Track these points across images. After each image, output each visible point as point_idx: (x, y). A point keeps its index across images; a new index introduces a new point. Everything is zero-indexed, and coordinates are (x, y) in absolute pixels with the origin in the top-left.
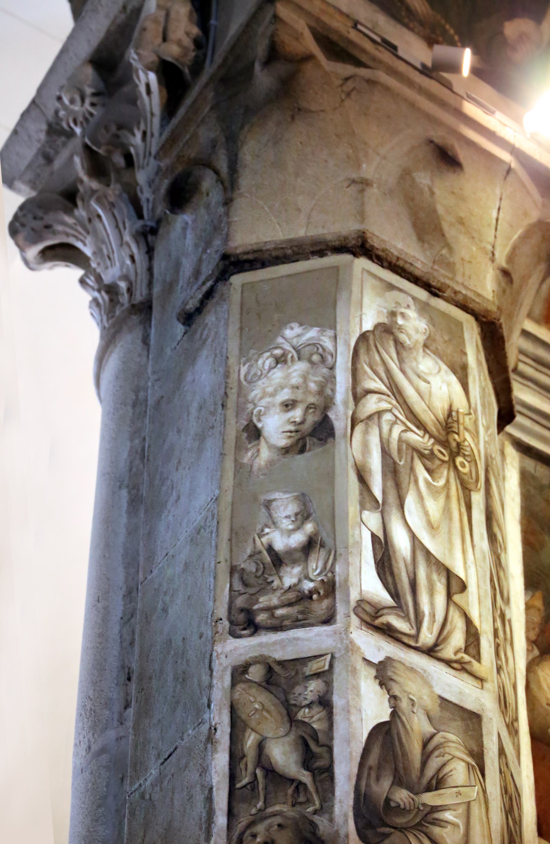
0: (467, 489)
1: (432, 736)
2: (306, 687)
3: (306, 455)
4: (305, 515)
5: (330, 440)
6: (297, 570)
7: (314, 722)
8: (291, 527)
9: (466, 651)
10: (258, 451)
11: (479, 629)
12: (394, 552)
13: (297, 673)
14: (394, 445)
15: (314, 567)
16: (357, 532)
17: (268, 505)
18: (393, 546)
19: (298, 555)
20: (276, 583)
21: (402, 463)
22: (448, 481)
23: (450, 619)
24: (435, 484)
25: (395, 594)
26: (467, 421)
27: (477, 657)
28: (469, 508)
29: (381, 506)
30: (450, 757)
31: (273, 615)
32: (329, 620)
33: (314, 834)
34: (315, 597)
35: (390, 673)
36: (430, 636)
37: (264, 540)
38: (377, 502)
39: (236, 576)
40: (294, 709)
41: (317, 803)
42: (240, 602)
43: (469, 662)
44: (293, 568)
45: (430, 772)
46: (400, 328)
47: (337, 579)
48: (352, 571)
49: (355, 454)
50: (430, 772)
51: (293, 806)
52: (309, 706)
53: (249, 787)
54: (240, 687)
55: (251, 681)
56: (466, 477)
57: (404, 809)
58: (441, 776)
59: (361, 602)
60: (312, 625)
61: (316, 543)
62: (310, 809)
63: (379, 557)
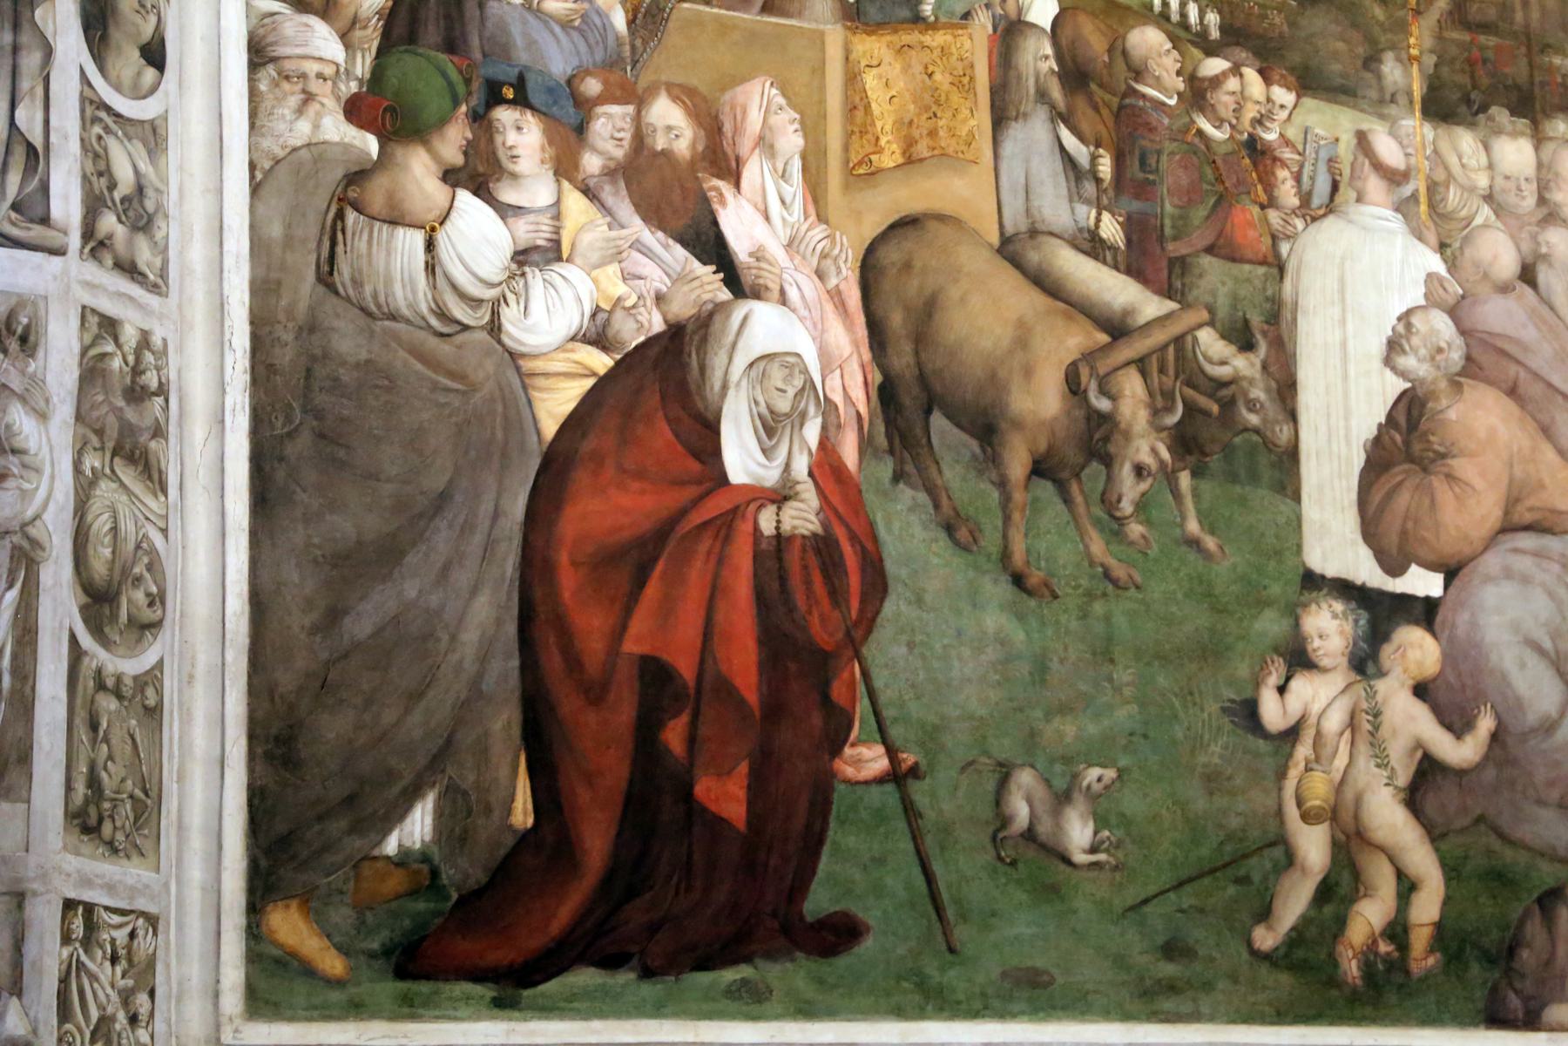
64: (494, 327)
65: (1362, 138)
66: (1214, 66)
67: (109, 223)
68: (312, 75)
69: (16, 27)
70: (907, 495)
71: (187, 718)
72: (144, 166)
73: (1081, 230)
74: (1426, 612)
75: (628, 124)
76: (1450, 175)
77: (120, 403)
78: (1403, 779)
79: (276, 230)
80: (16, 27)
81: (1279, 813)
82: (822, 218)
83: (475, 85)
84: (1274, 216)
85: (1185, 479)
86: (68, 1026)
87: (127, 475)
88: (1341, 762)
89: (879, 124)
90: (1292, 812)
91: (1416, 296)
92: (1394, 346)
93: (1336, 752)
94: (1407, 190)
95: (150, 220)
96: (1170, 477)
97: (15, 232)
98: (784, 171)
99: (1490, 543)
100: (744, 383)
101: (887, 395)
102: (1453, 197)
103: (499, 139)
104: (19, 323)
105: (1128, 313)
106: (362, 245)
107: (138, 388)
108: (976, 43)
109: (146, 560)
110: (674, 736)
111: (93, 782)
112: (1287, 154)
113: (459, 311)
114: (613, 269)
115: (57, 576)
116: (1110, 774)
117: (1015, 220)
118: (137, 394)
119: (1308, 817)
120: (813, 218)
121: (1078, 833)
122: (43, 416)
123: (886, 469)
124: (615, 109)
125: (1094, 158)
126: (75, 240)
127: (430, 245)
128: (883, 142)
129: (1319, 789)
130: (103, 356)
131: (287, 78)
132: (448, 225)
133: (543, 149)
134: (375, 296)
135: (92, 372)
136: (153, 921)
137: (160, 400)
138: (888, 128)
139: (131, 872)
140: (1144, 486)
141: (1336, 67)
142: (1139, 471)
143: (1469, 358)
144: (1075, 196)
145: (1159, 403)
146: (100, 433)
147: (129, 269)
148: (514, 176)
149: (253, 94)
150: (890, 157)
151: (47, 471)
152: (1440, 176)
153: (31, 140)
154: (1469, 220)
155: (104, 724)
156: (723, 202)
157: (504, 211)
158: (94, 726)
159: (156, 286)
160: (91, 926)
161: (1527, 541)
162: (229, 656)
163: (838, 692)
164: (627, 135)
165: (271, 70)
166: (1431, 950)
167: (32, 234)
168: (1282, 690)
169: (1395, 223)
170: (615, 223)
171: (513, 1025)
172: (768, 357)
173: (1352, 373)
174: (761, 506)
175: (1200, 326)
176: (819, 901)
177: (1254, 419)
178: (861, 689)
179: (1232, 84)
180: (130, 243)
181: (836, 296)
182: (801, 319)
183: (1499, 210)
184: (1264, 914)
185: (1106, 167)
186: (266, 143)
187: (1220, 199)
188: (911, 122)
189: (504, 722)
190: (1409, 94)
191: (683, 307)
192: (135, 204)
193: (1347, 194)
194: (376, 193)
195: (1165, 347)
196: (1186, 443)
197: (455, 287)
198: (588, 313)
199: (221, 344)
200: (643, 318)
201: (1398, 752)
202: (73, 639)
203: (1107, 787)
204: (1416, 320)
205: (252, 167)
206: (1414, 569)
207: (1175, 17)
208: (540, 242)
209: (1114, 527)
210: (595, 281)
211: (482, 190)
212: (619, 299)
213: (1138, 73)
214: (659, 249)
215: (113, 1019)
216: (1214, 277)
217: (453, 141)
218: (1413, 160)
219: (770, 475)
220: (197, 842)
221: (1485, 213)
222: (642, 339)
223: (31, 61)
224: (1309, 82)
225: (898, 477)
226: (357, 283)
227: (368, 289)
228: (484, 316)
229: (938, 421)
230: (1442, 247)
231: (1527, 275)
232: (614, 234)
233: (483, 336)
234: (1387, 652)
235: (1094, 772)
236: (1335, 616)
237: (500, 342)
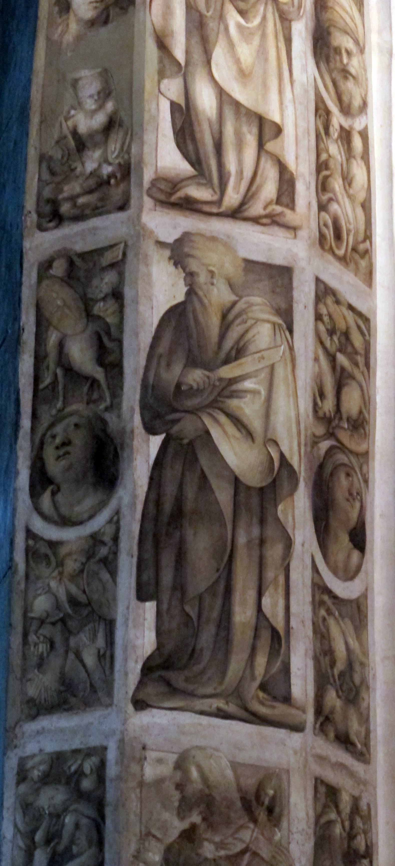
0: (287, 19)
1: (234, 304)
2: (102, 279)
3: (110, 26)
4: (107, 92)
5: (131, 8)
6: (97, 154)
7: (108, 315)
8: (94, 107)
9: (278, 201)
10: (68, 25)
11: (295, 174)
12: (197, 115)
13: (95, 265)
15: (113, 149)
16: (154, 106)
17: (75, 83)
18: (195, 109)
19: (99, 138)
20: (79, 169)
21: (209, 14)
22: (264, 18)
23: (260, 172)
24: (249, 25)
27: (291, 205)
29: (183, 69)
30: (253, 322)
31: (75, 205)
32: (123, 207)
33: (104, 431)
34: (112, 181)
35: (186, 250)
36: (236, 196)
37: (70, 123)
38: (179, 64)
39: (44, 165)
40: (91, 303)
41: (108, 400)
42: (47, 193)
43: (281, 214)
44: (94, 152)
45: (229, 343)
47: (133, 160)
48: (146, 149)
49: (154, 19)
50: (229, 343)
51: (88, 403)
52: (104, 299)
53: (50, 387)
54: (45, 283)
55: (55, 277)
56: (286, 8)
57: (198, 390)
58: (242, 343)
59: (154, 183)
60: (109, 212)
61: (115, 122)
62: (102, 407)
63: (178, 127)
69: (262, 522)
80: (262, 522)
95: (357, 693)
97: (263, 710)
104: (266, 794)
107: (352, 852)
126: (310, 717)
130: (330, 823)
153: (274, 624)
159: (362, 754)
167: (276, 712)
180: (346, 717)
192: (347, 678)
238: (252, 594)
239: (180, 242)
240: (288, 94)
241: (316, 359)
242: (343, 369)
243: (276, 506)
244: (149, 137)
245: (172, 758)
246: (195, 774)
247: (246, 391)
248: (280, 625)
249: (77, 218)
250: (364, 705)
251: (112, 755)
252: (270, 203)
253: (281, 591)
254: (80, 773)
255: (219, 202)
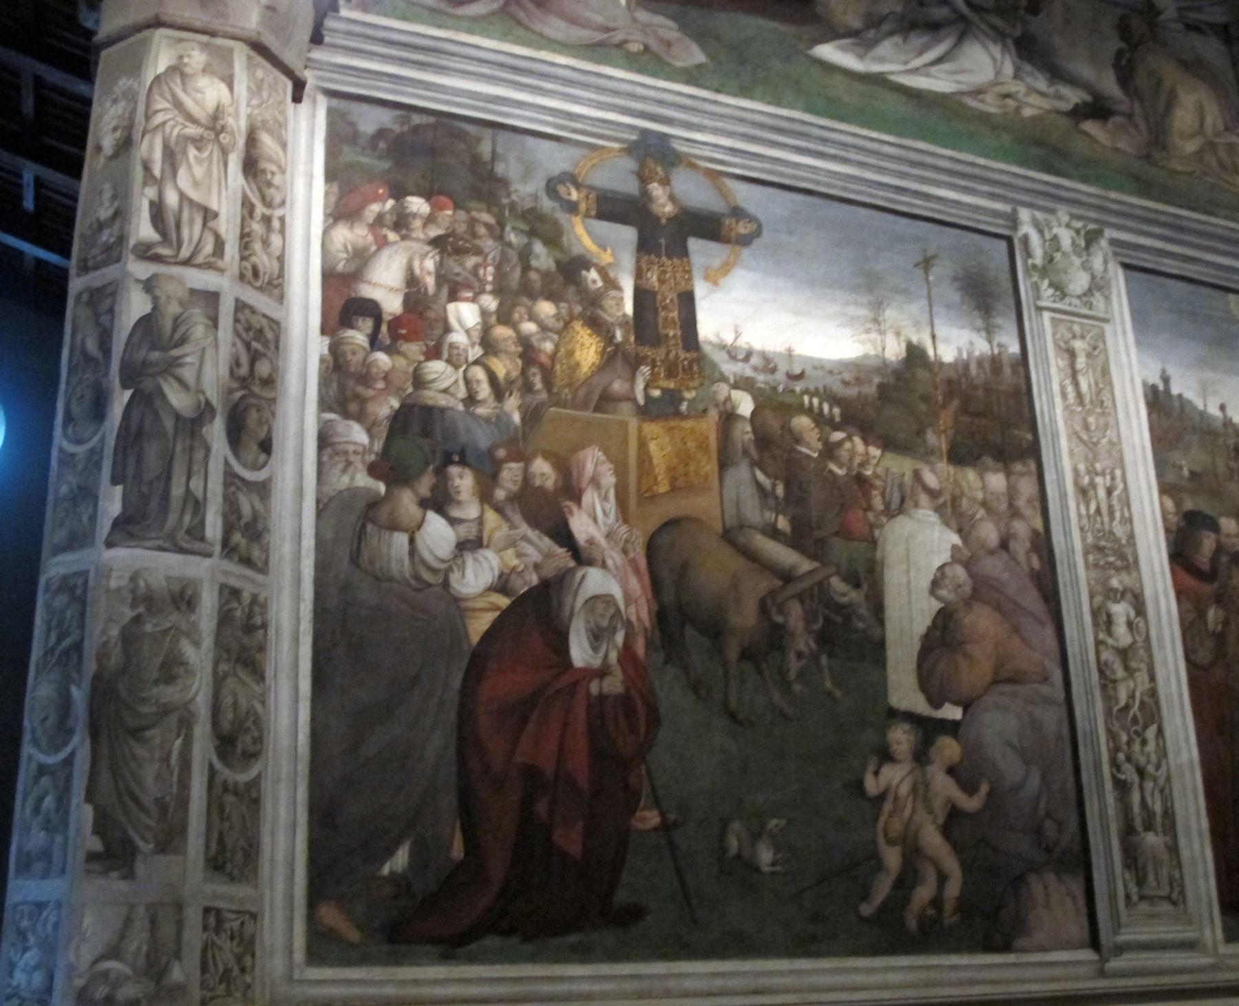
14: (173, 140)
17: (101, 192)
25: (164, 233)
26: (231, 110)
28: (226, 164)
46: (186, 65)
50: (178, 336)
60: (111, 264)
64: (446, 585)
65: (917, 476)
66: (838, 436)
67: (237, 538)
68: (351, 452)
70: (671, 671)
71: (276, 800)
72: (258, 506)
73: (767, 524)
74: (952, 728)
75: (520, 473)
76: (962, 492)
77: (240, 634)
78: (941, 821)
79: (329, 535)
81: (874, 842)
82: (626, 521)
83: (438, 455)
84: (871, 516)
85: (824, 660)
86: (207, 976)
87: (244, 675)
88: (907, 812)
89: (657, 470)
90: (881, 840)
91: (945, 557)
92: (935, 585)
93: (905, 806)
94: (941, 500)
96: (815, 658)
97: (186, 545)
98: (606, 496)
99: (986, 690)
100: (583, 611)
101: (661, 616)
102: (965, 503)
103: (450, 483)
105: (793, 568)
106: (375, 541)
108: (709, 426)
109: (252, 719)
110: (541, 808)
111: (221, 842)
112: (878, 483)
113: (427, 576)
114: (510, 552)
115: (202, 731)
116: (783, 822)
117: (731, 520)
118: (249, 628)
119: (891, 842)
120: (620, 521)
121: (765, 856)
122: (197, 644)
123: (659, 658)
124: (513, 465)
125: (774, 486)
126: (218, 548)
127: (412, 541)
128: (659, 478)
129: (897, 827)
131: (338, 454)
132: (422, 531)
133: (473, 487)
134: (381, 569)
135: (224, 619)
136: (254, 916)
137: (261, 632)
138: (662, 472)
139: (241, 891)
140: (803, 662)
141: (902, 436)
142: (799, 655)
143: (975, 590)
144: (764, 506)
145: (809, 618)
146: (228, 651)
147: (247, 561)
148: (459, 503)
149: (320, 464)
150: (663, 488)
151: (198, 676)
152: (957, 492)
154: (974, 515)
155: (227, 810)
156: (571, 513)
157: (453, 522)
158: (222, 810)
160: (220, 921)
161: (1007, 688)
162: (300, 767)
163: (633, 780)
164: (520, 479)
165: (329, 450)
166: (955, 912)
168: (876, 773)
169: (934, 518)
170: (513, 526)
171: (451, 968)
172: (596, 597)
173: (913, 598)
174: (589, 682)
175: (832, 575)
176: (622, 896)
177: (861, 625)
178: (645, 780)
179: (847, 445)
181: (633, 563)
182: (615, 576)
183: (989, 510)
184: (865, 897)
185: (780, 490)
186: (326, 489)
187: (842, 506)
188: (674, 468)
189: (447, 802)
190: (940, 449)
191: (549, 571)
193: (909, 503)
194: (383, 514)
195: (811, 588)
196: (824, 639)
197: (424, 562)
198: (497, 573)
199: (298, 598)
200: (527, 577)
201: (938, 804)
202: (211, 766)
203: (781, 830)
204: (947, 570)
205: (318, 502)
206: (947, 705)
207: (816, 410)
208: (471, 538)
209: (785, 686)
210: (501, 558)
211: (441, 510)
212: (514, 569)
213: (798, 440)
214: (536, 539)
215: (231, 970)
216: (840, 550)
217: (425, 485)
218: (943, 485)
219: (597, 662)
220: (281, 870)
221: (981, 512)
222: (526, 589)
223: (199, 455)
224: (888, 444)
225: (667, 661)
226: (371, 562)
227: (378, 566)
228: (439, 579)
229: (689, 631)
230: (960, 531)
231: (1004, 545)
232: (512, 532)
233: (438, 590)
234: (933, 750)
235: (774, 822)
236: (905, 732)
237: (448, 592)
238: (184, 479)
239: (149, 280)
240: (224, 194)
241: (234, 345)
242: (256, 351)
243: (202, 428)
244: (134, 221)
245: (127, 575)
246: (142, 583)
247: (187, 363)
248: (199, 495)
249: (96, 268)
250: (266, 541)
251: (92, 575)
252: (208, 256)
253: (202, 476)
254: (75, 586)
255: (177, 256)
